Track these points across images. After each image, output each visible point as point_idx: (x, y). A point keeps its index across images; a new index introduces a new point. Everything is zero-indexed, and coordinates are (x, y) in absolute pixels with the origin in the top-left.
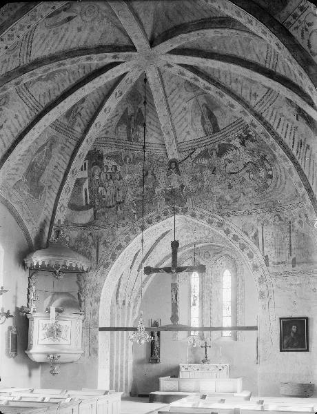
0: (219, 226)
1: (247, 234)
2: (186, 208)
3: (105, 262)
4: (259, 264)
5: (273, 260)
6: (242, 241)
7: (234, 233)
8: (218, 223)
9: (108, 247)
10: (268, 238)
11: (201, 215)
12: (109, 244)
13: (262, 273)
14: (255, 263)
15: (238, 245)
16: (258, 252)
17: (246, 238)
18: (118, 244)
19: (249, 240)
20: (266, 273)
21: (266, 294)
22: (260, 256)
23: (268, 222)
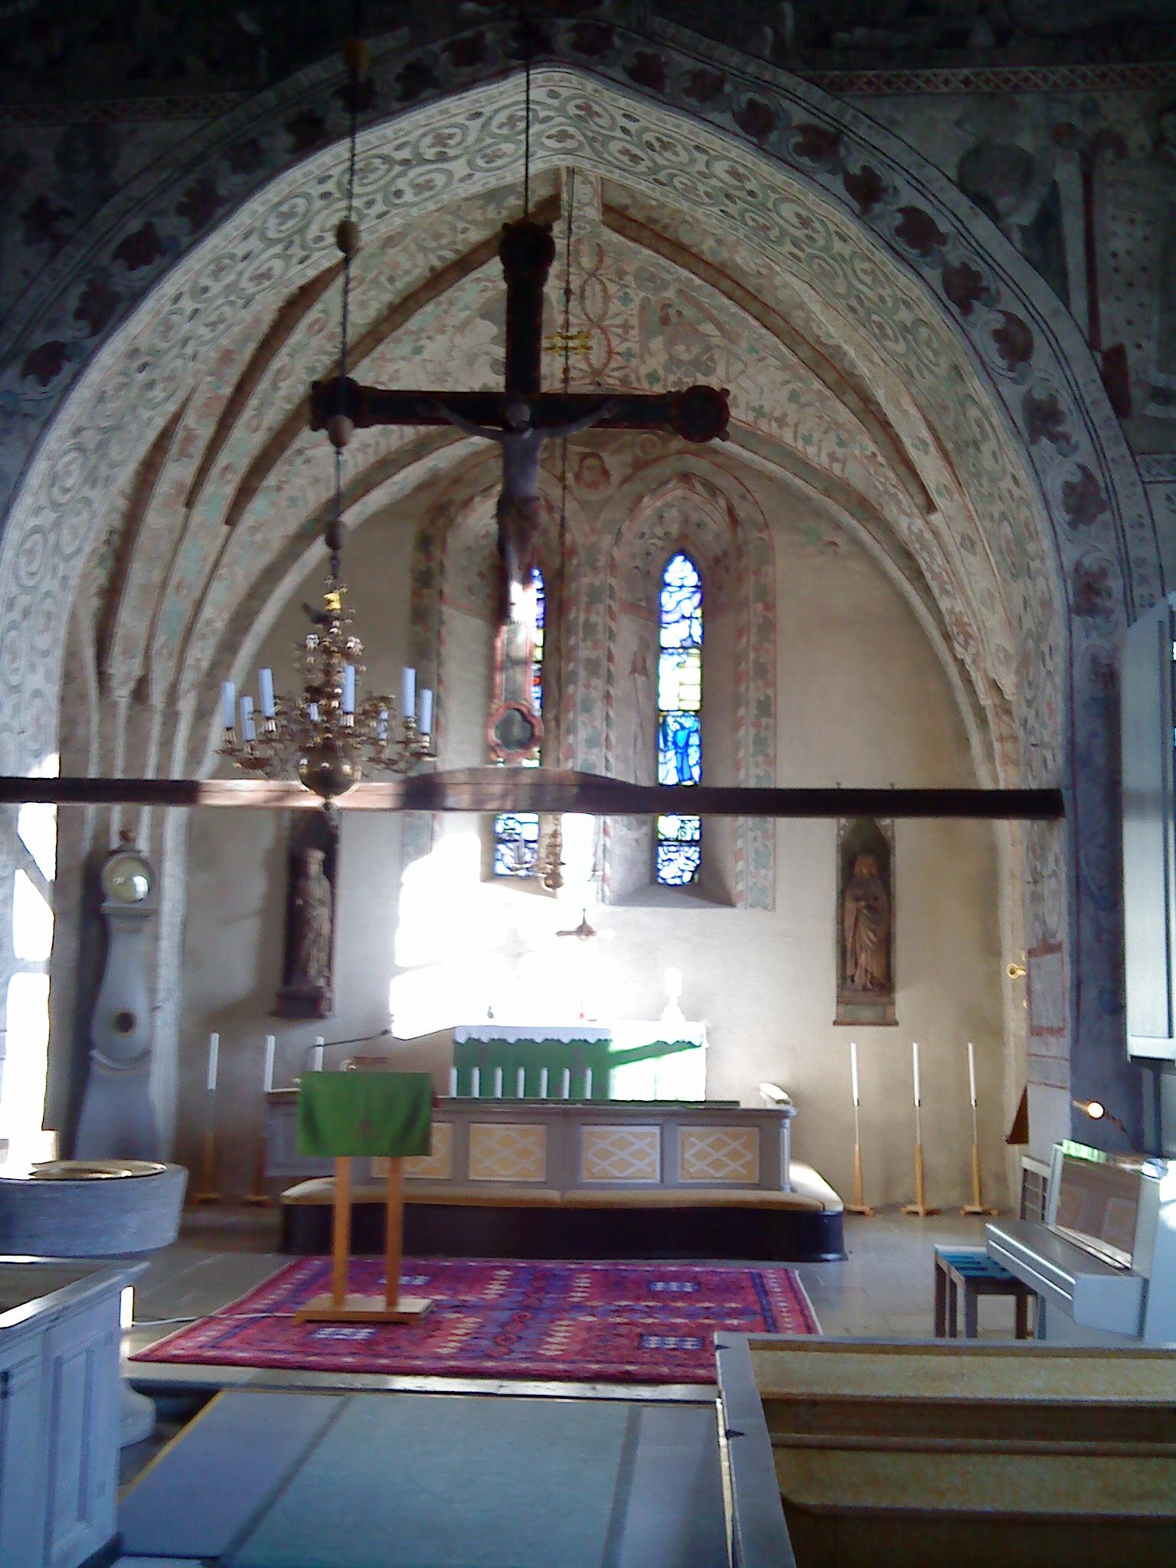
0: (801, 150)
1: (984, 203)
2: (606, 33)
3: (39, 339)
4: (1065, 403)
5: (1160, 380)
6: (955, 254)
7: (908, 197)
8: (805, 130)
9: (60, 241)
10: (1122, 238)
11: (698, 77)
12: (65, 226)
13: (1085, 454)
14: (1040, 394)
15: (934, 275)
16: (1062, 326)
17: (982, 227)
18: (134, 225)
19: (997, 247)
20: (1117, 451)
21: (1115, 584)
22: (1074, 344)
23: (1120, 146)
